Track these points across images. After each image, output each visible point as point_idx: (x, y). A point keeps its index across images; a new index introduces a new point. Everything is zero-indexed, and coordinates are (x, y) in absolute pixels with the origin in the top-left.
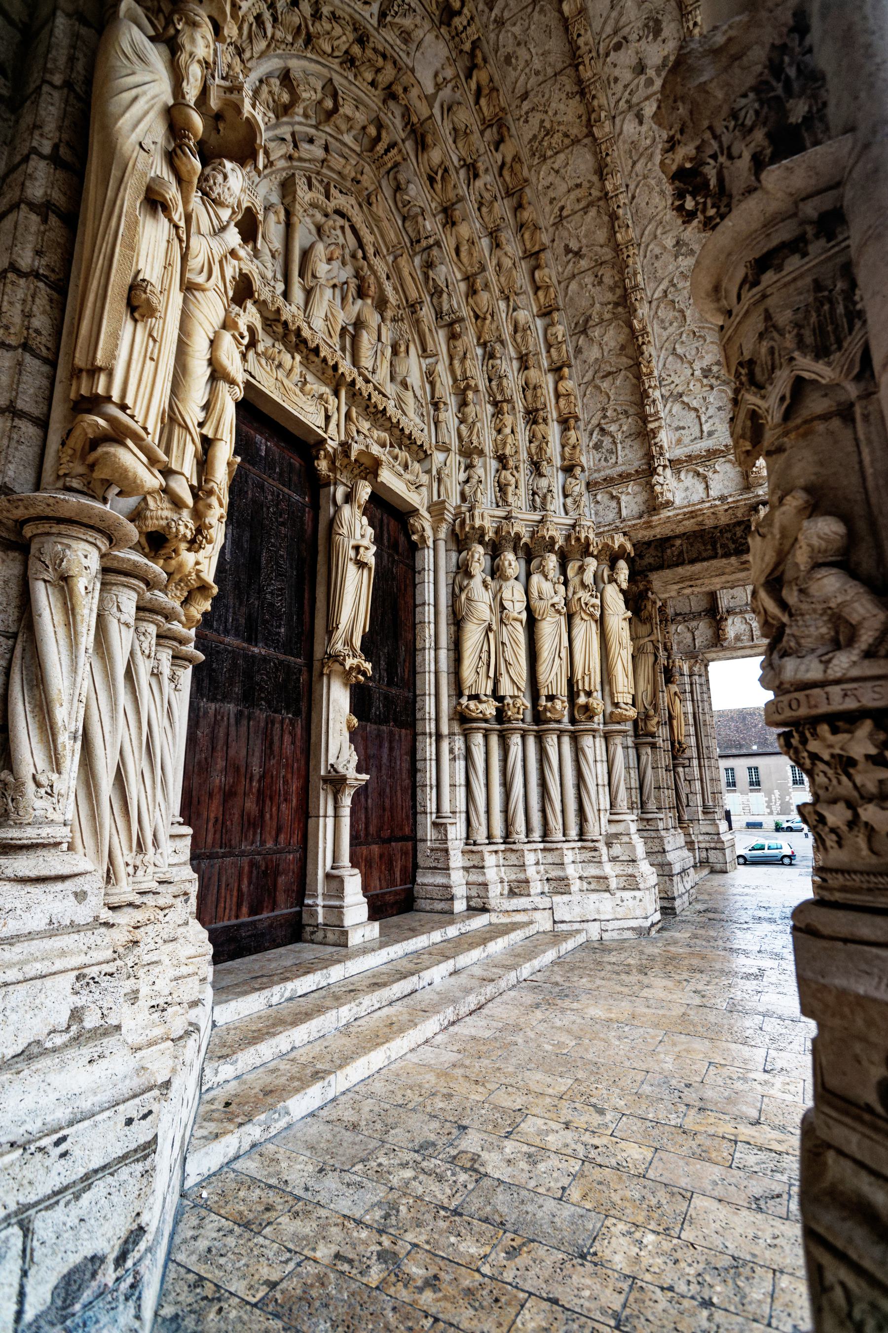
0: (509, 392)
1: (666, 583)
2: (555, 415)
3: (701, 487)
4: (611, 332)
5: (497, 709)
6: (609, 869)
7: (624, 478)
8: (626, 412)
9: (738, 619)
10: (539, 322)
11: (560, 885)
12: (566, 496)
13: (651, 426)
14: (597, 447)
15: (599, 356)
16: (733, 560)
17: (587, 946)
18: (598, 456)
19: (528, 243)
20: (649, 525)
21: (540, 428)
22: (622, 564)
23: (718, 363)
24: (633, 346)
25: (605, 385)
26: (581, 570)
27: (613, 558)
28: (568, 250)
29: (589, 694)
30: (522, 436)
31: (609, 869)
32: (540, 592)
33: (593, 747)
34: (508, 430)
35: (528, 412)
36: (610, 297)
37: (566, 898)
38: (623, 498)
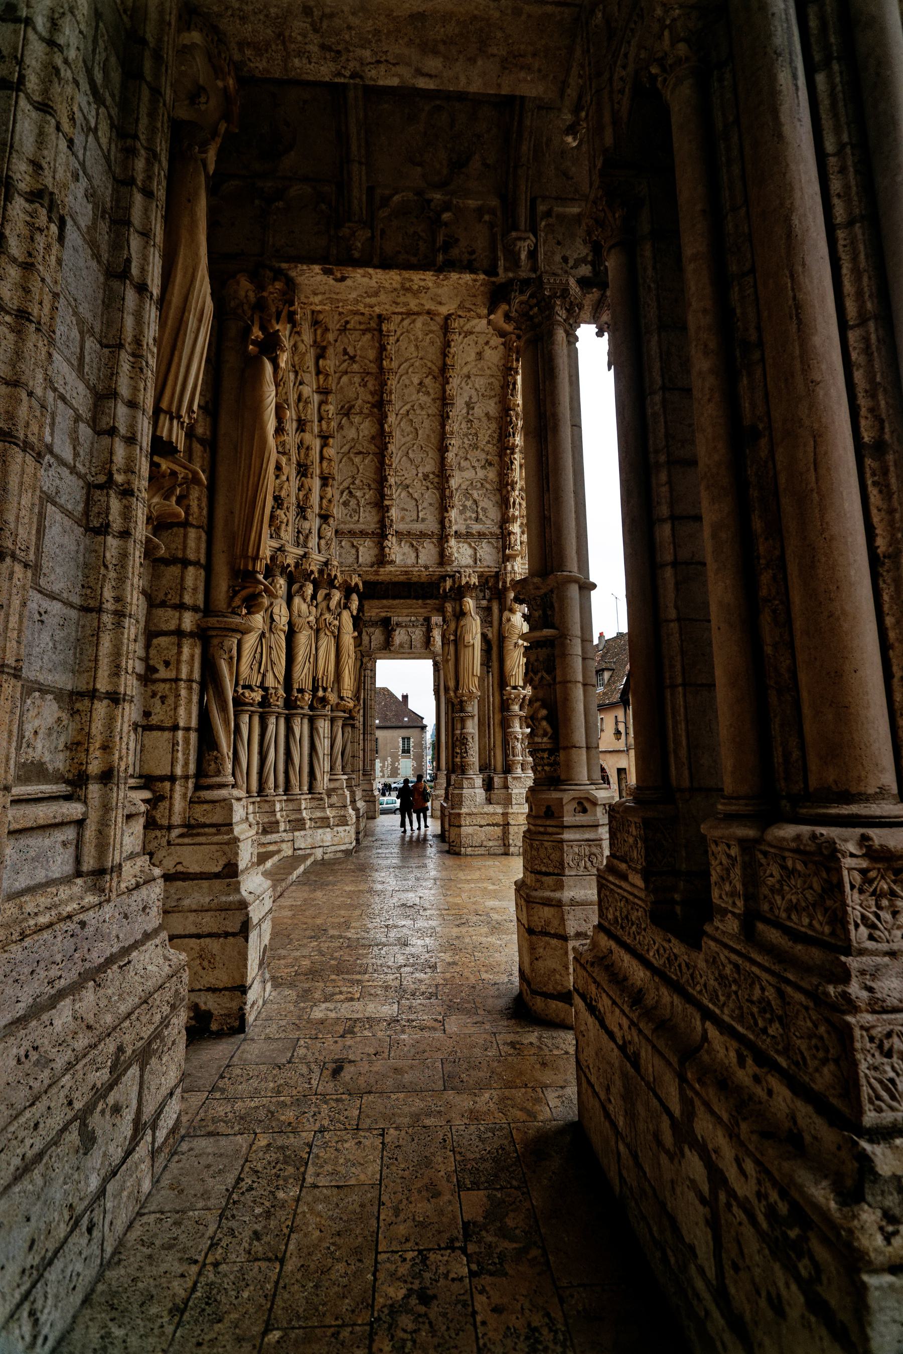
0: (287, 447)
1: (372, 607)
2: (318, 472)
3: (413, 555)
4: (367, 424)
5: (262, 697)
6: (329, 813)
7: (363, 534)
8: (369, 485)
9: (403, 631)
10: (316, 398)
11: (298, 824)
12: (320, 538)
13: (387, 503)
14: (346, 504)
15: (355, 437)
16: (420, 602)
17: (315, 862)
18: (345, 512)
19: (319, 337)
20: (377, 573)
21: (307, 481)
22: (355, 597)
23: (433, 473)
24: (381, 439)
25: (357, 460)
26: (328, 597)
27: (348, 591)
28: (345, 352)
29: (325, 690)
30: (294, 484)
31: (329, 813)
32: (299, 611)
33: (323, 726)
34: (284, 478)
35: (299, 464)
36: (369, 398)
37: (302, 833)
38: (361, 548)
